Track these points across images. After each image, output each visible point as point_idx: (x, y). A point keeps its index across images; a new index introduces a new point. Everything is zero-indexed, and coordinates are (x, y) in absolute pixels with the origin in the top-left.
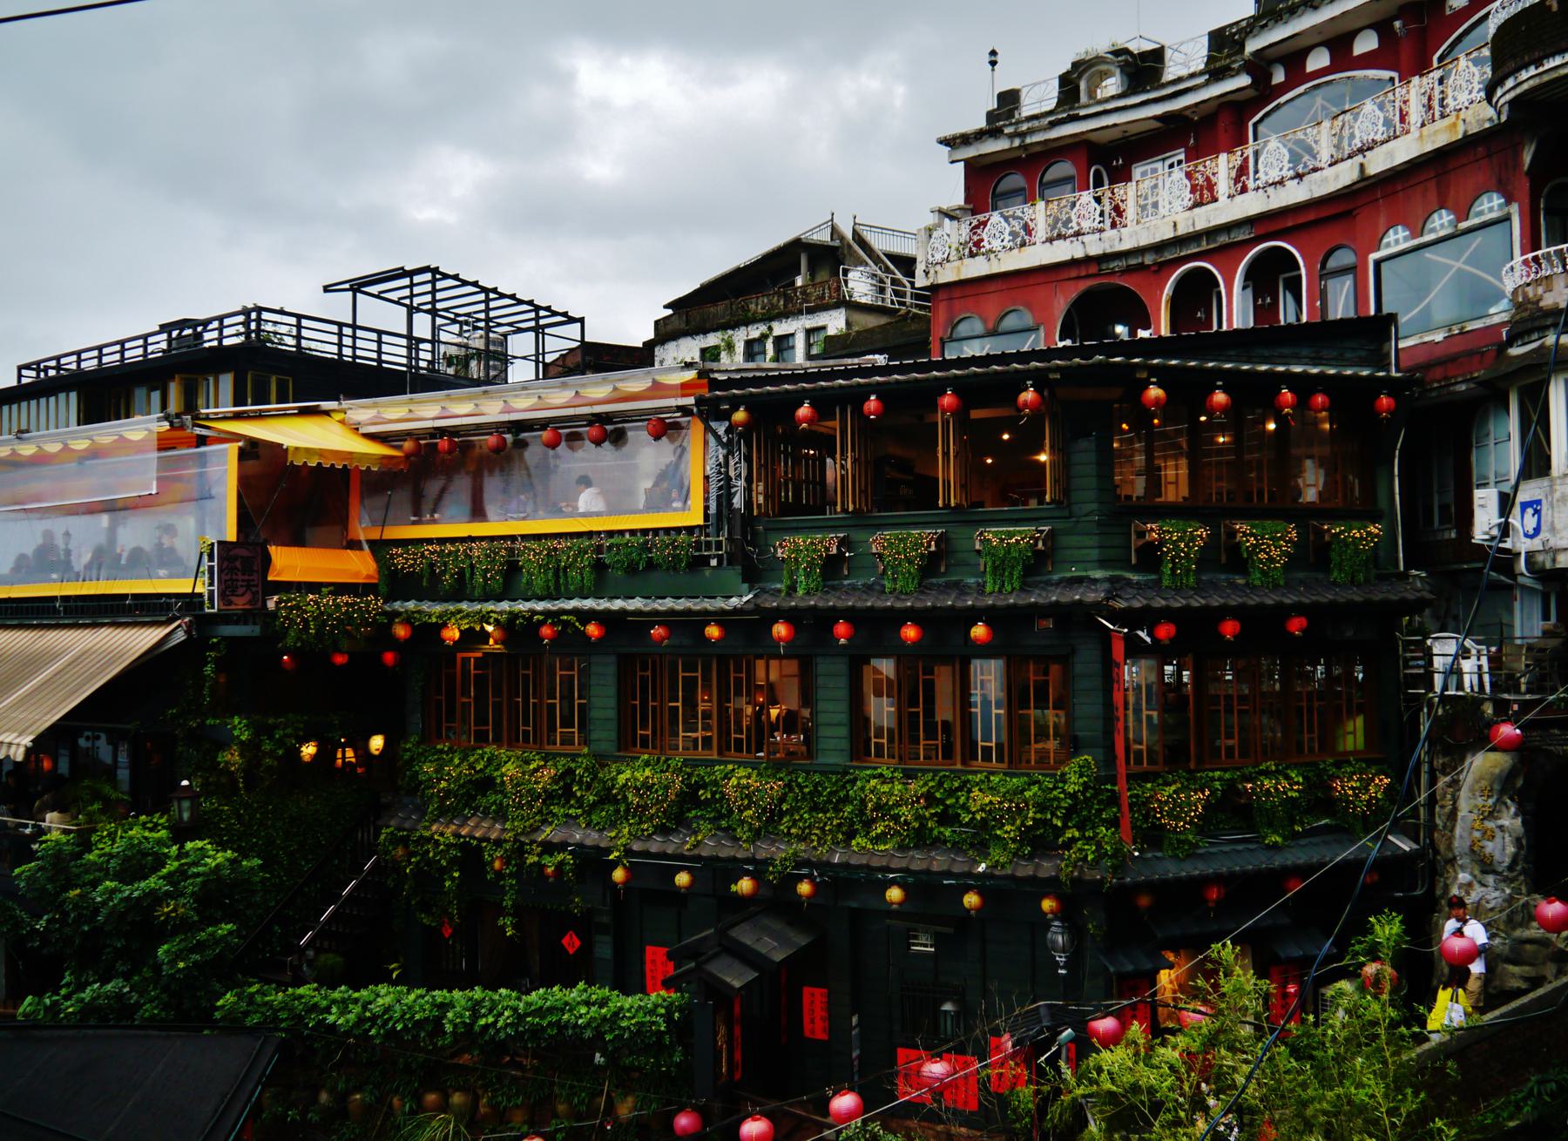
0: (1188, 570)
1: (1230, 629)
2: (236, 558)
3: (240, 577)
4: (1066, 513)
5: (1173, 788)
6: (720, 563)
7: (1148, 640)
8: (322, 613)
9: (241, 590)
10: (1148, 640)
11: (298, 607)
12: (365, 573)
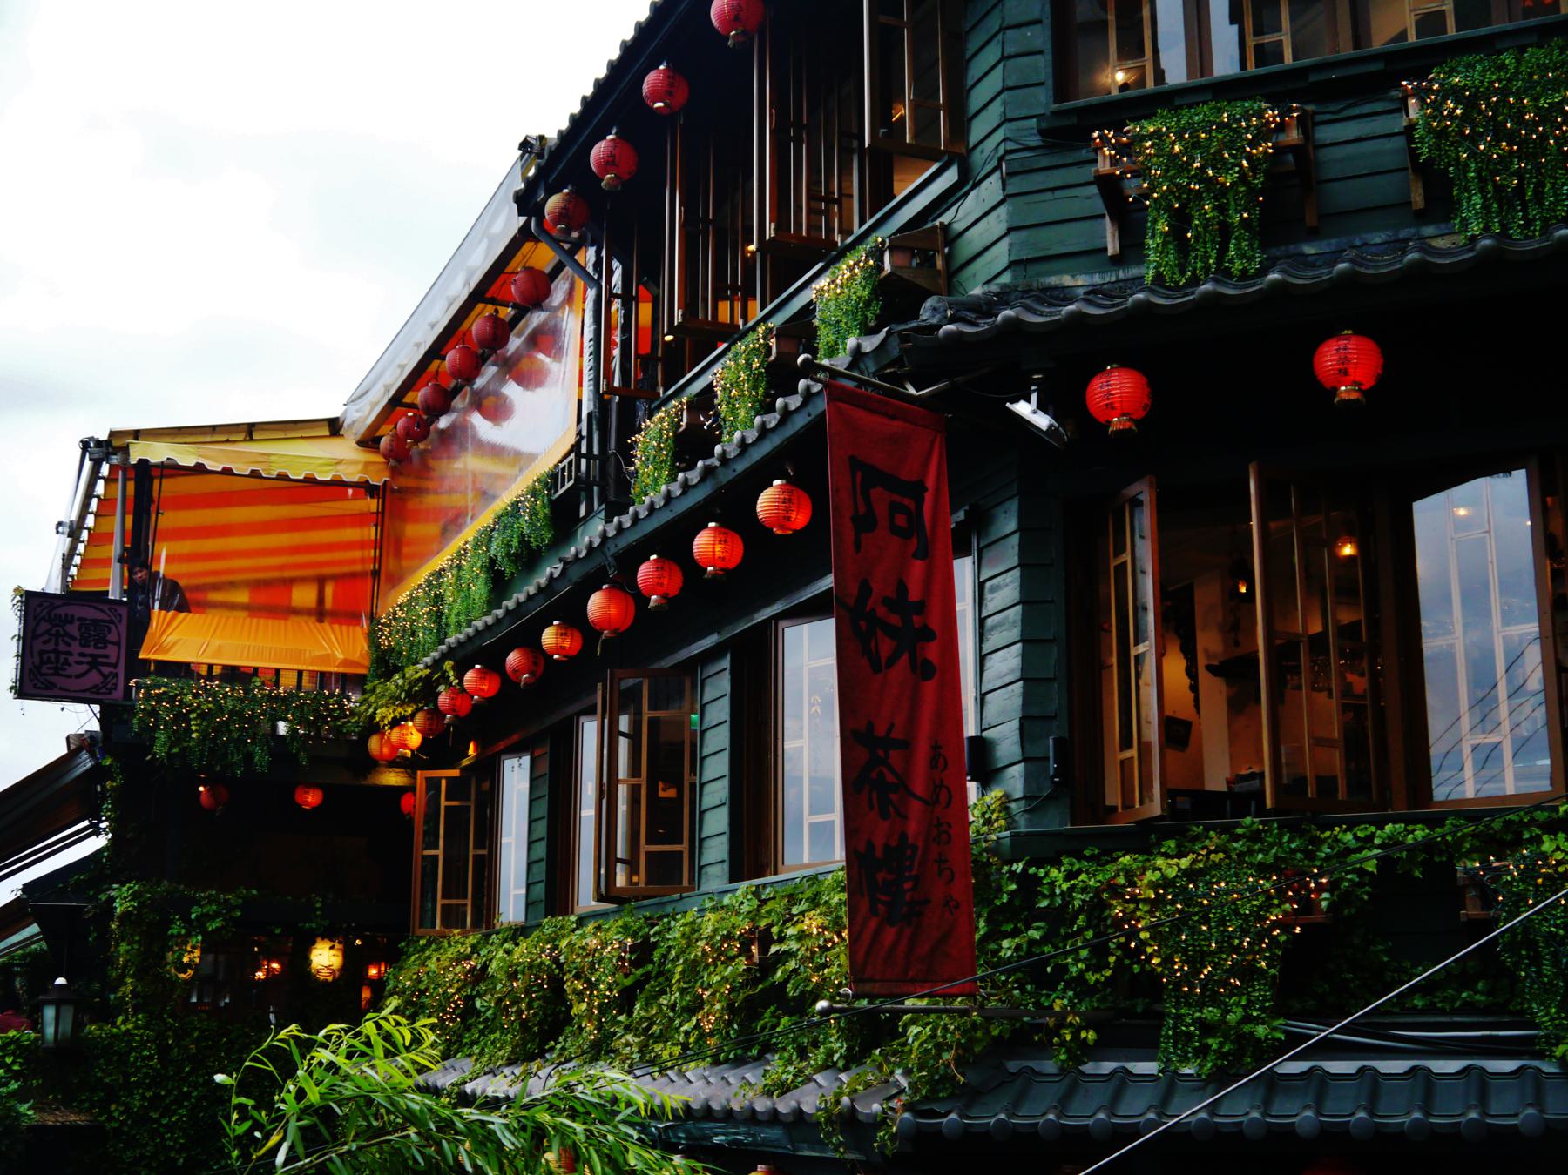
0: (1225, 232)
1: (1346, 364)
2: (70, 620)
3: (76, 647)
4: (951, 176)
5: (1185, 863)
6: (590, 510)
7: (1042, 421)
8: (220, 709)
9: (76, 669)
10: (1042, 421)
11: (172, 699)
12: (340, 656)
